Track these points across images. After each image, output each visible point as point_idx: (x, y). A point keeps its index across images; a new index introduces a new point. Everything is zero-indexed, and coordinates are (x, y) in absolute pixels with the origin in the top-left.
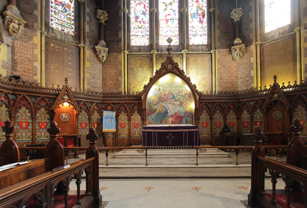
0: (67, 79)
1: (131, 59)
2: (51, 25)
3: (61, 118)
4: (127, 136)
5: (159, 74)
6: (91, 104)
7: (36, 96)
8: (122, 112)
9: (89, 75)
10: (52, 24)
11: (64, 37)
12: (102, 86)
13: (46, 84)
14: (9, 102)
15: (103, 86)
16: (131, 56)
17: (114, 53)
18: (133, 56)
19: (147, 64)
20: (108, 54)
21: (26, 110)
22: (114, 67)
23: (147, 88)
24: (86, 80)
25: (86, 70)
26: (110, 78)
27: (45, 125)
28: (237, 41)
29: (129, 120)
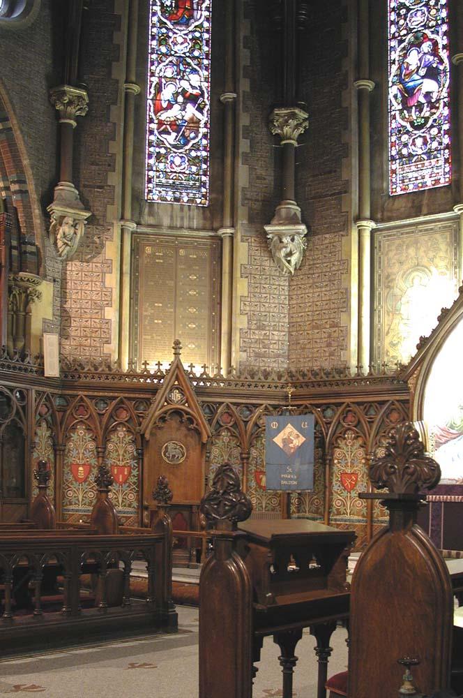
0: (180, 343)
1: (385, 244)
2: (148, 194)
3: (165, 454)
4: (360, 518)
6: (250, 411)
7: (105, 396)
8: (349, 435)
9: (245, 318)
10: (150, 191)
11: (179, 219)
12: (286, 348)
13: (130, 363)
14: (53, 415)
15: (289, 350)
16: (385, 233)
17: (327, 236)
18: (394, 232)
19: (442, 254)
20: (308, 241)
21: (85, 435)
22: (325, 284)
23: (428, 347)
24: (236, 337)
25: (237, 305)
26: (313, 320)
27: (126, 473)
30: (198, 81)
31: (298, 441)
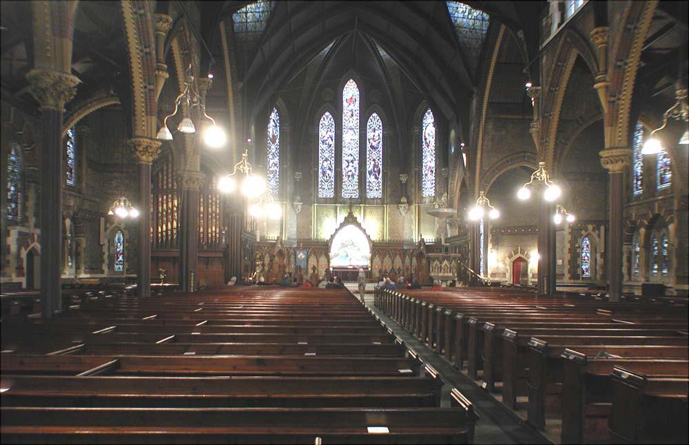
5: (342, 225)
23: (333, 237)
24: (287, 230)
28: (404, 200)
29: (318, 262)
30: (276, 160)
31: (303, 257)
